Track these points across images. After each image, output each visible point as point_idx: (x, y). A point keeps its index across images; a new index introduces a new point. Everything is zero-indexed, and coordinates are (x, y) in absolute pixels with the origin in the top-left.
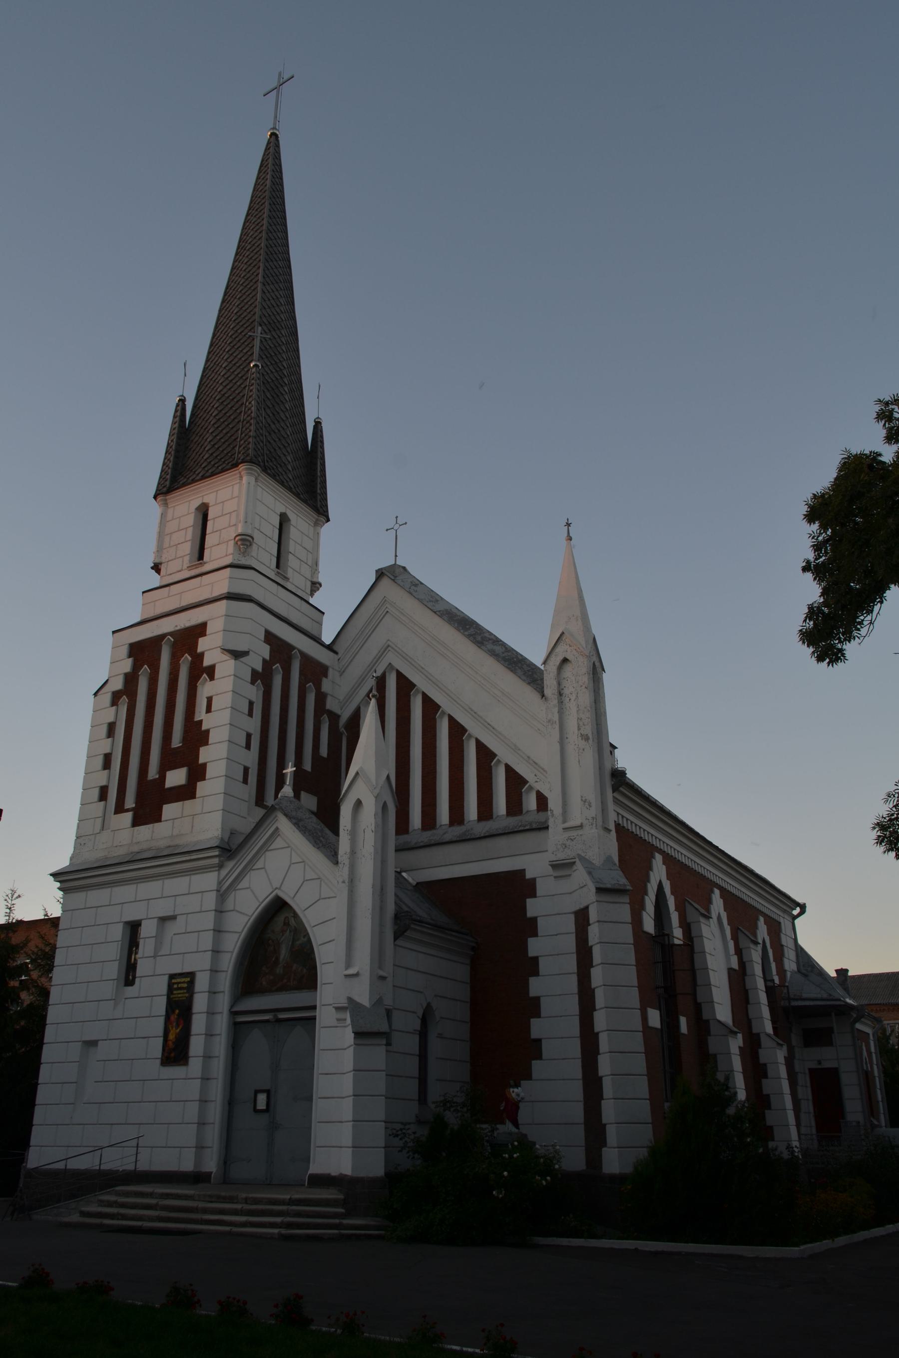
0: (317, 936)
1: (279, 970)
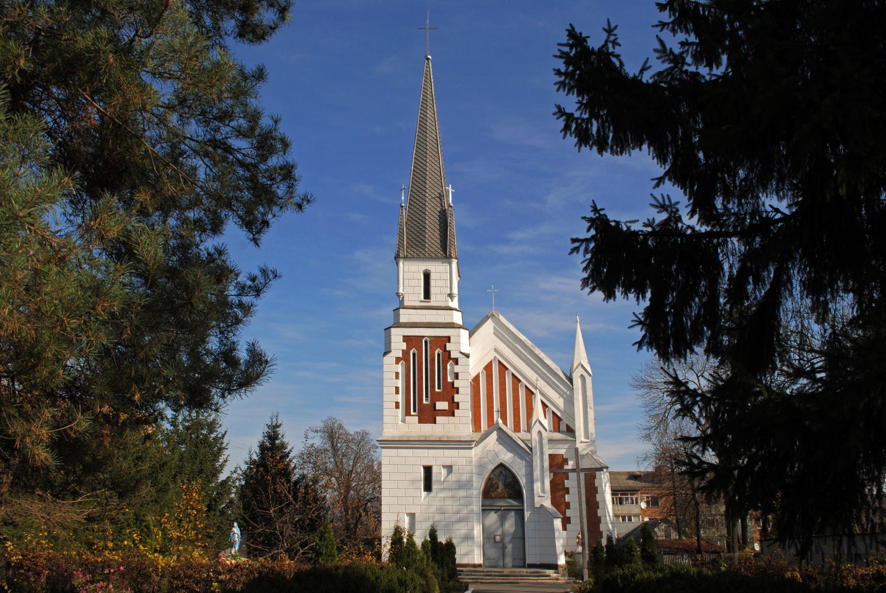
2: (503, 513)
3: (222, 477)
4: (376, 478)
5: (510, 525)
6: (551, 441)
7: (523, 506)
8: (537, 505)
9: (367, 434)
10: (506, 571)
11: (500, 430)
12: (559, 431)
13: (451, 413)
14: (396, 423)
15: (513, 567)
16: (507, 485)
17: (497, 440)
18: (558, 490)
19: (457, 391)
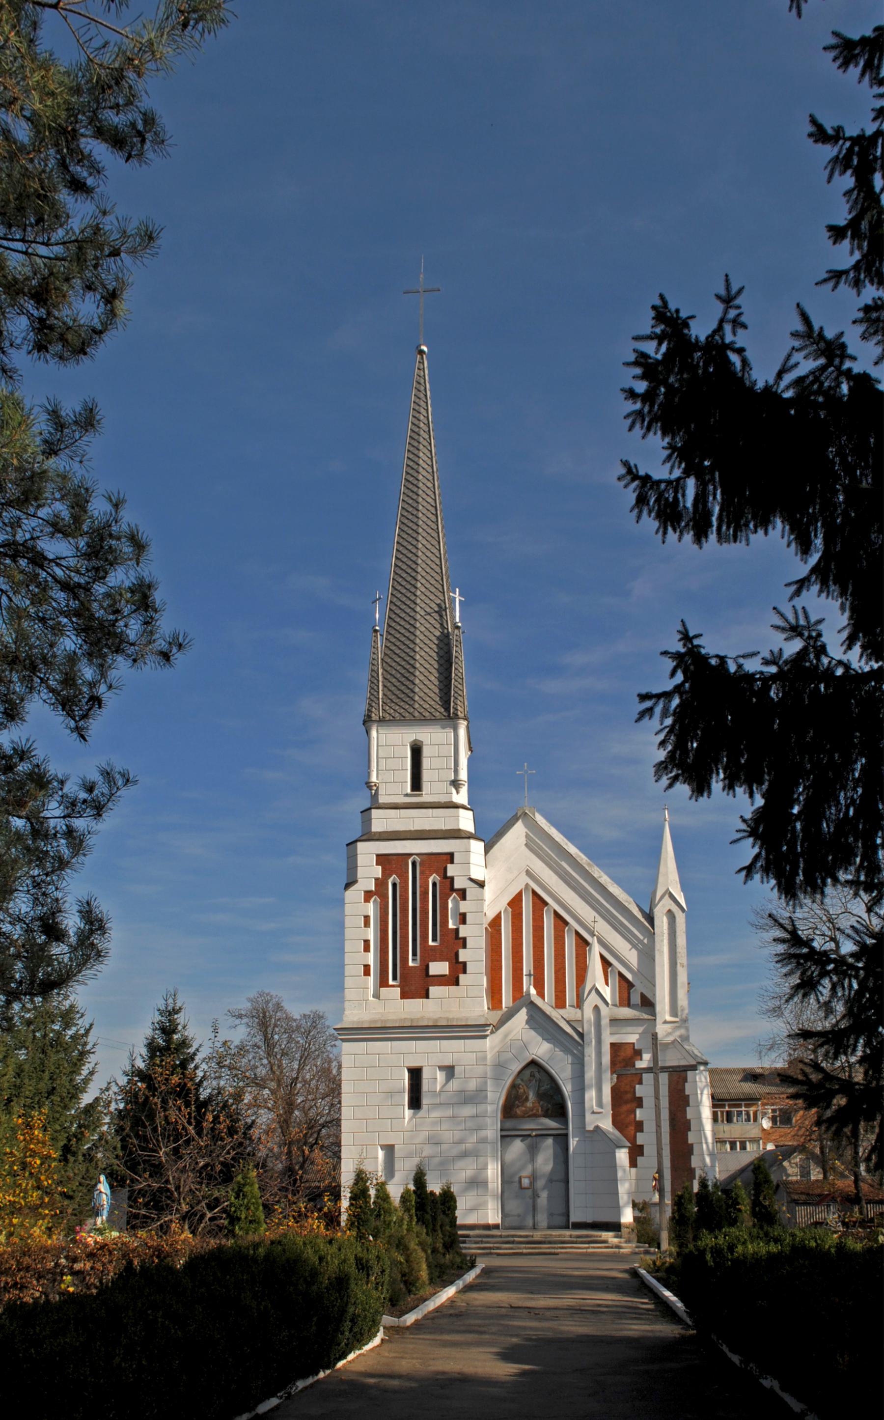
2: (533, 1141)
3: (86, 1099)
4: (334, 1090)
5: (545, 1161)
6: (615, 1021)
7: (567, 1128)
8: (590, 1127)
9: (321, 1017)
10: (538, 1235)
11: (532, 1005)
12: (629, 1005)
14: (365, 999)
15: (550, 1227)
16: (541, 1096)
17: (527, 1022)
18: (624, 1101)
19: (464, 943)
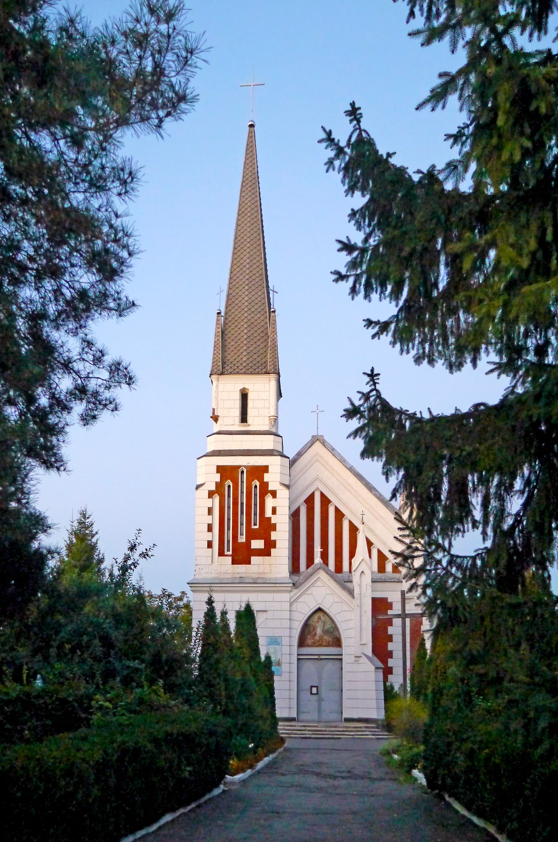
0: (341, 627)
1: (317, 638)
13: (266, 552)
19: (274, 527)
